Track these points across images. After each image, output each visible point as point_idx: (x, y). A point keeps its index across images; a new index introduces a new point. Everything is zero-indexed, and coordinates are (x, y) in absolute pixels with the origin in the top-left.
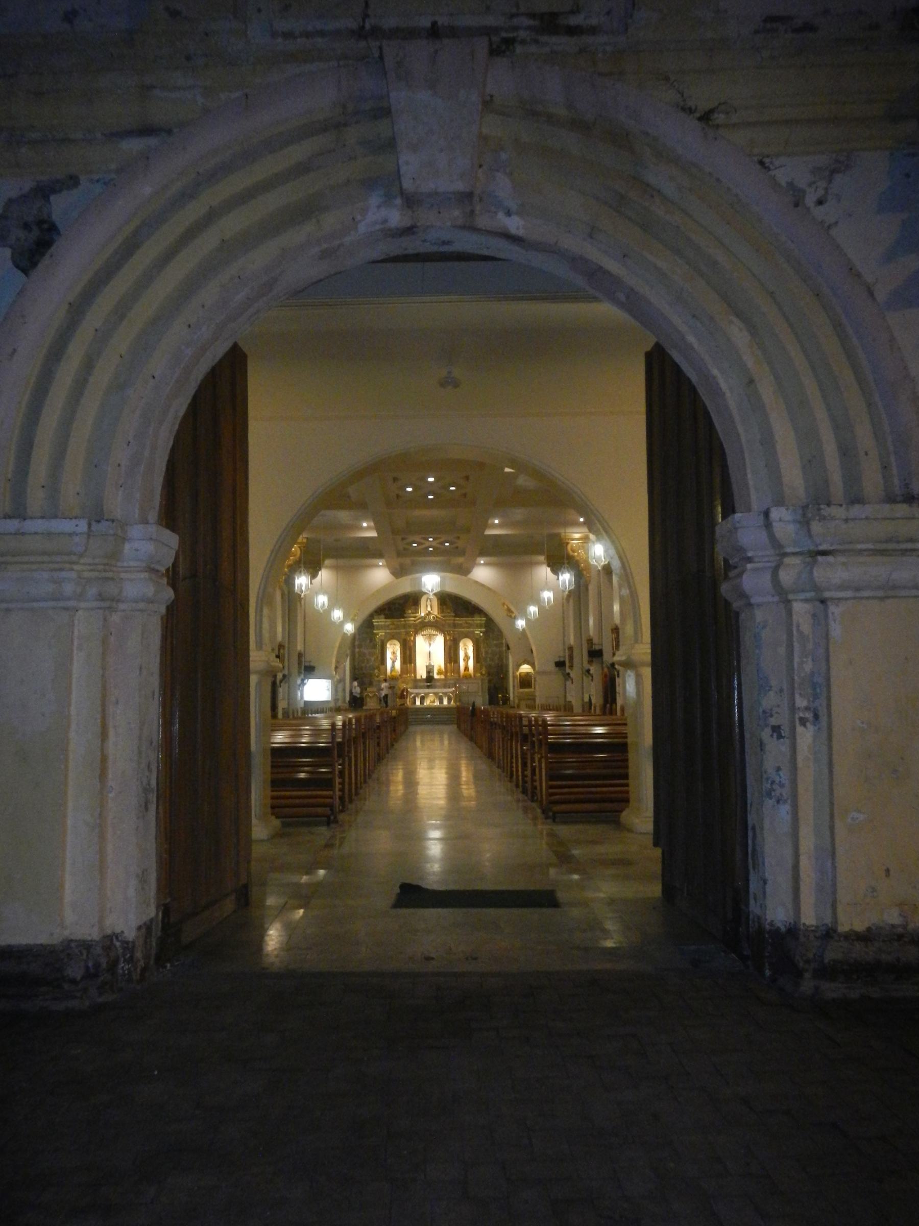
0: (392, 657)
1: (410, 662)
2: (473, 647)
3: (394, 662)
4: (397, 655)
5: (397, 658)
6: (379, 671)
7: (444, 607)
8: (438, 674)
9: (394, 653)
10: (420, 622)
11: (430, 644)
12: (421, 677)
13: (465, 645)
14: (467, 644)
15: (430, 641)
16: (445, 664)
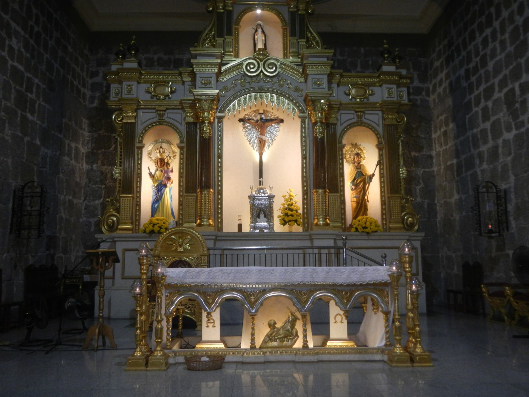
0: (158, 173)
1: (208, 187)
2: (380, 148)
3: (160, 188)
4: (170, 168)
5: (171, 175)
6: (118, 210)
7: (303, 42)
8: (284, 223)
9: (162, 163)
10: (235, 79)
11: (262, 144)
12: (240, 226)
13: (355, 145)
14: (359, 143)
15: (261, 134)
16: (305, 193)
